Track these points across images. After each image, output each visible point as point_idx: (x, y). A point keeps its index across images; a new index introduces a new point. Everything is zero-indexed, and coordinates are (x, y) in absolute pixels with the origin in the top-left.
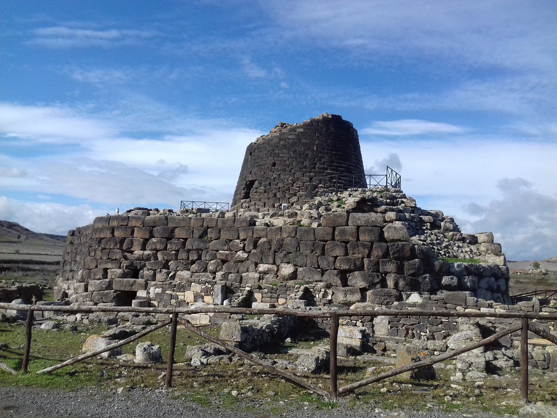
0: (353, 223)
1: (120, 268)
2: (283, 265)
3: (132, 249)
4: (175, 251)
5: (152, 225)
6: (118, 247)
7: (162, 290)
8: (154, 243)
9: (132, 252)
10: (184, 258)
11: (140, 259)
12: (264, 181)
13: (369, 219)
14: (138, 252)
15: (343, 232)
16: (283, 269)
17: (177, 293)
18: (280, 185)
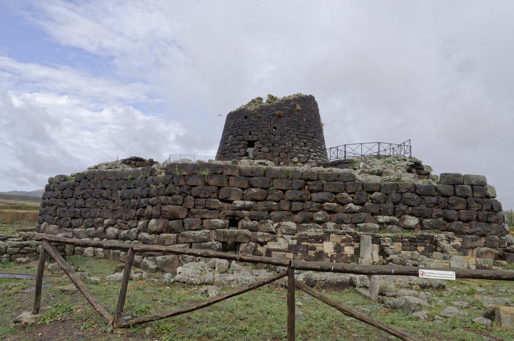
0: (468, 182)
1: (219, 218)
2: (407, 216)
3: (231, 199)
4: (276, 201)
5: (250, 174)
6: (215, 195)
7: (297, 241)
8: (254, 194)
9: (231, 202)
10: (286, 209)
11: (240, 209)
12: (267, 143)
13: (479, 180)
14: (239, 203)
15: (463, 189)
16: (408, 220)
17: (315, 244)
18: (283, 147)
